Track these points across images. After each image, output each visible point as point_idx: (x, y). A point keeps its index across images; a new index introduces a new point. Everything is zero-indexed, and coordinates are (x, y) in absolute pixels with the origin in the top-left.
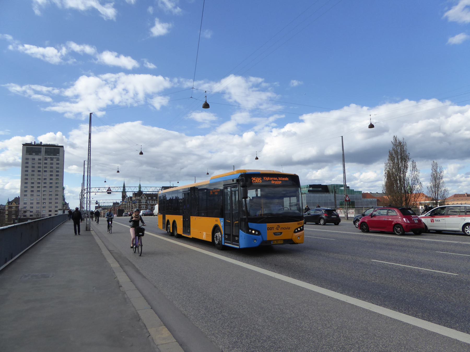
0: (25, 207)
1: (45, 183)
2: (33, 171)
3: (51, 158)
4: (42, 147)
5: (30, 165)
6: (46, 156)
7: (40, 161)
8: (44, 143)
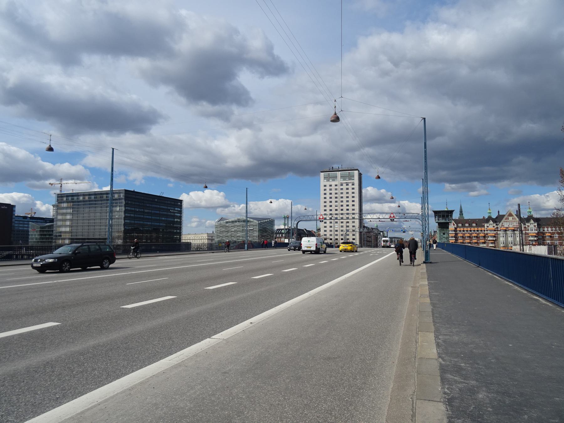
0: (325, 235)
2: (331, 198)
7: (336, 187)
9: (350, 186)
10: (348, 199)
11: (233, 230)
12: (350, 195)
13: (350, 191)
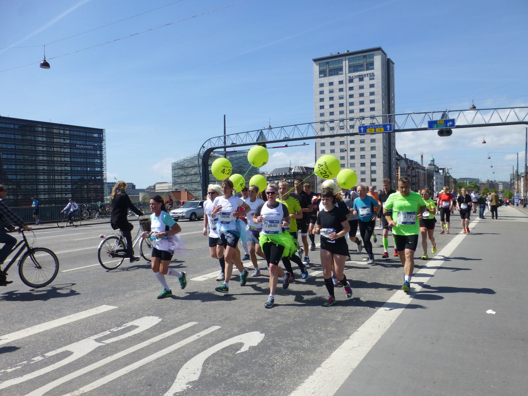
3: (359, 76)
5: (326, 95)
6: (352, 75)
7: (341, 86)
8: (351, 51)
10: (362, 107)
11: (193, 172)
12: (367, 98)
13: (367, 91)
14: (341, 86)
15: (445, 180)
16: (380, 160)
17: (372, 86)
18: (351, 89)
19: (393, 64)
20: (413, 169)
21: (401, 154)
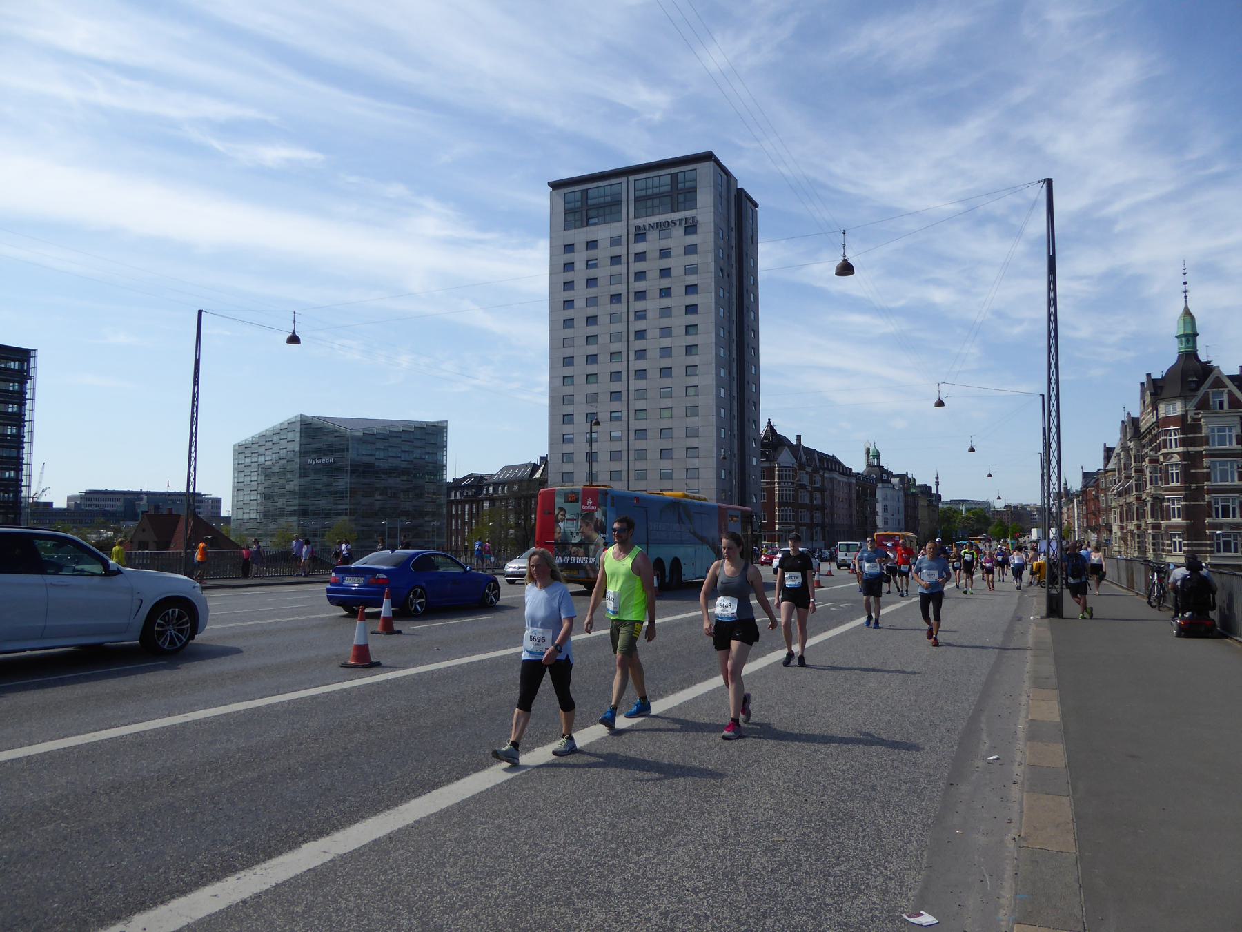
1: (640, 354)
3: (661, 226)
4: (624, 180)
5: (580, 274)
9: (678, 239)
13: (677, 263)
14: (616, 251)
15: (906, 502)
16: (708, 441)
17: (691, 250)
18: (640, 256)
19: (756, 205)
20: (815, 471)
21: (787, 430)
